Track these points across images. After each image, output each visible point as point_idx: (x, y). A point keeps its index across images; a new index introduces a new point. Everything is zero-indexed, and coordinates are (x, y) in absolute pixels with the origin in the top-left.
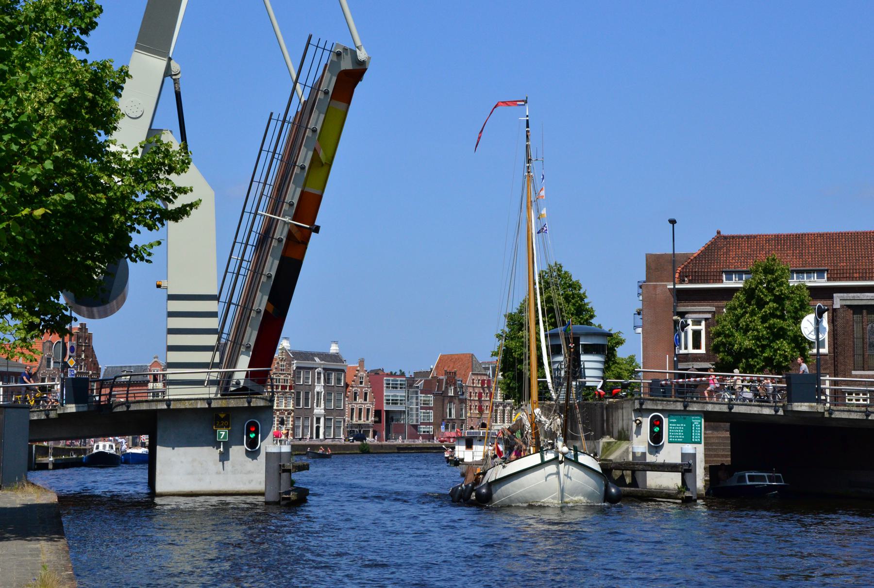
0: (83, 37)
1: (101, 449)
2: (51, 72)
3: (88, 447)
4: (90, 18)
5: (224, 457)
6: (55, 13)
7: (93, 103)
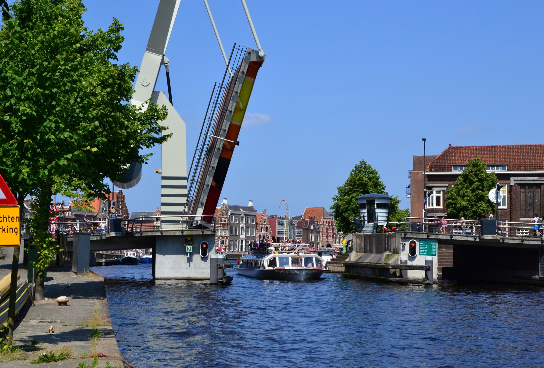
0: (115, 53)
1: (129, 255)
2: (100, 72)
3: (122, 254)
4: (118, 43)
5: (190, 260)
6: (102, 42)
7: (120, 85)
